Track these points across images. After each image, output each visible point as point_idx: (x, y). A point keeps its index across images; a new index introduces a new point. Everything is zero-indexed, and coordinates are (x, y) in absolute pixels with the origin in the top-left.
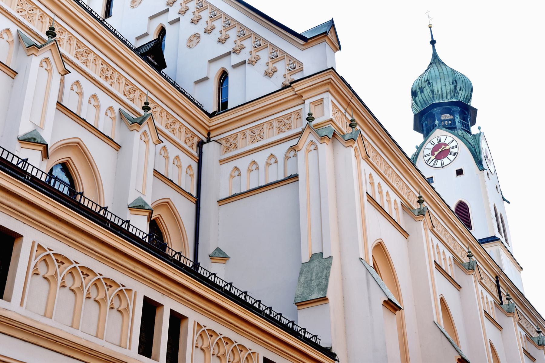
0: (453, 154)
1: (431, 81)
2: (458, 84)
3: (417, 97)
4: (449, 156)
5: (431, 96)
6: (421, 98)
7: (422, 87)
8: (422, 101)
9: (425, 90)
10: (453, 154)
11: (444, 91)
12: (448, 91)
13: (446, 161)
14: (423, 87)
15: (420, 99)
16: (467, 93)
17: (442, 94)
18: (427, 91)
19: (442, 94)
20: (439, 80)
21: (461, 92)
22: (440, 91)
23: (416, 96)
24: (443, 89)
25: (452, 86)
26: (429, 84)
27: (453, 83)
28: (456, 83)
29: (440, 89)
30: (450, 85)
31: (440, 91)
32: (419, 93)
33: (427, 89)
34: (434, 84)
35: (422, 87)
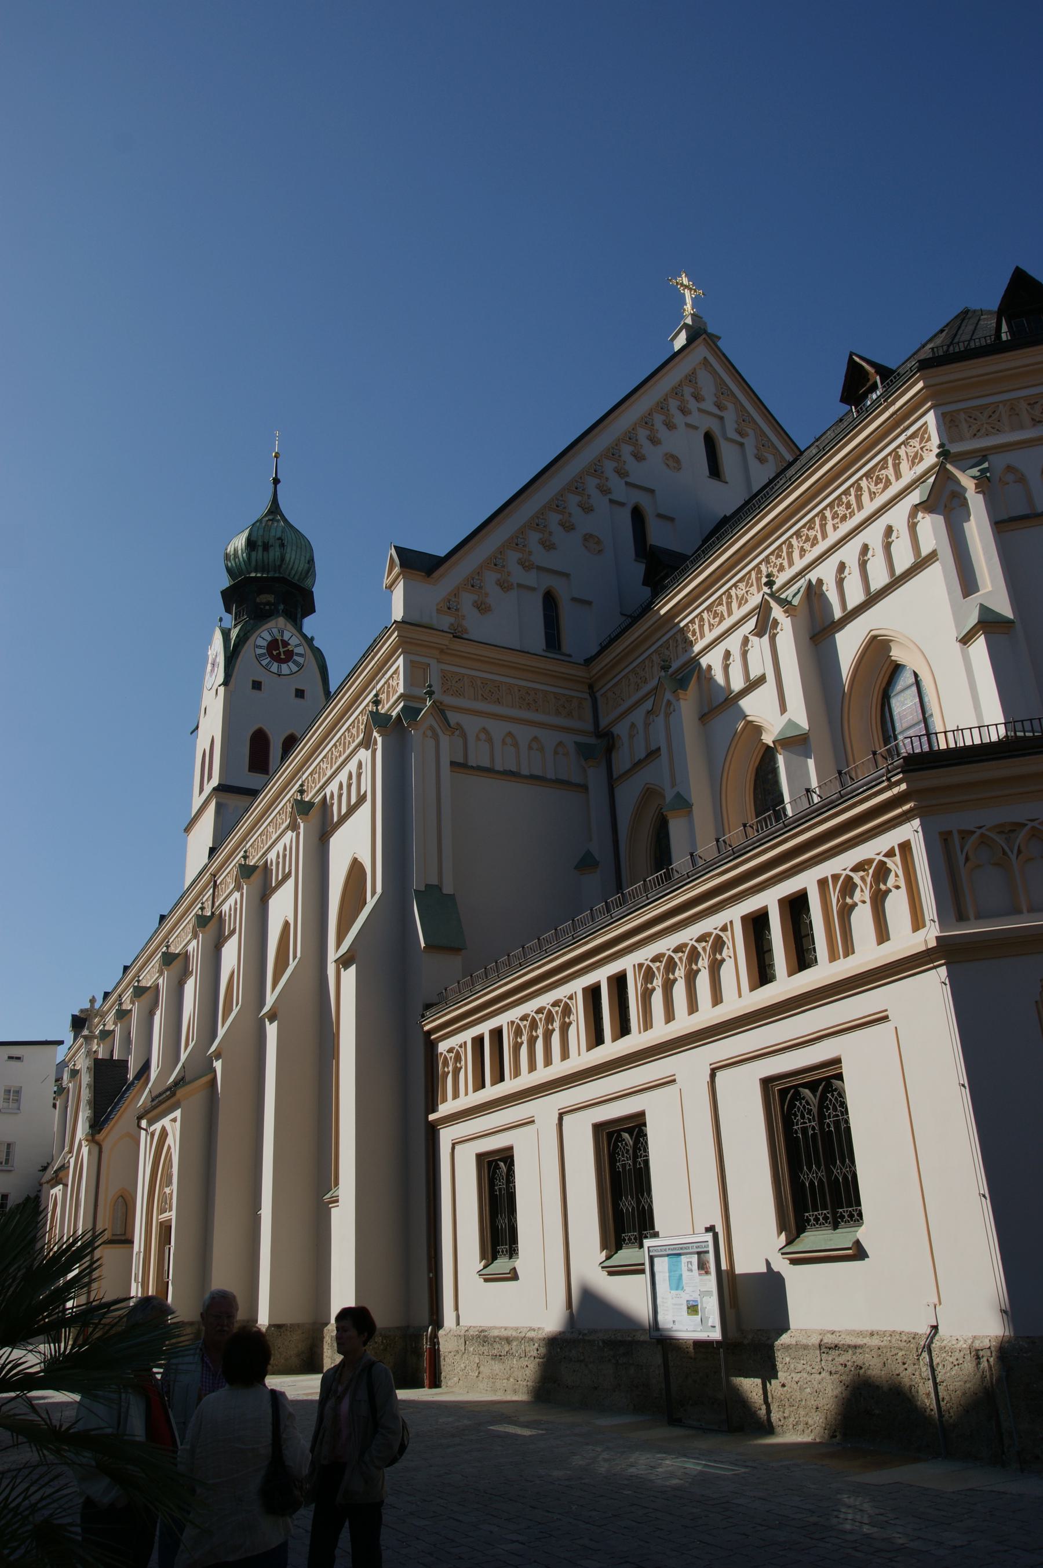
0: (296, 663)
4: (290, 664)
5: (278, 563)
6: (261, 557)
9: (271, 550)
10: (296, 663)
11: (296, 567)
12: (300, 569)
13: (285, 669)
14: (270, 543)
15: (258, 558)
17: (292, 568)
18: (274, 553)
19: (292, 568)
20: (294, 548)
22: (291, 563)
25: (307, 565)
26: (282, 545)
27: (309, 562)
29: (292, 560)
30: (305, 562)
31: (291, 563)
35: (268, 542)
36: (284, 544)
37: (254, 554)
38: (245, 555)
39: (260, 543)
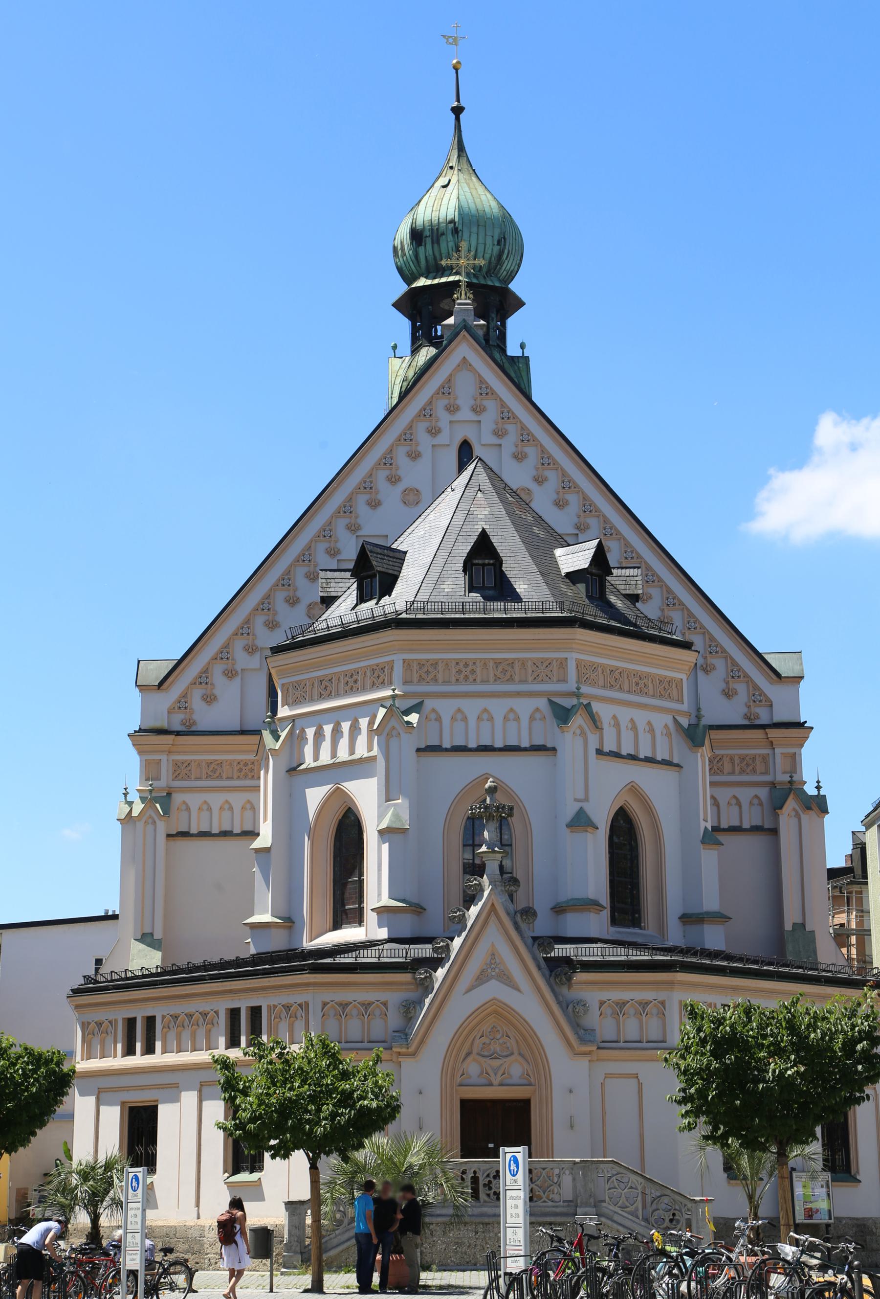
1: (460, 228)
2: (507, 247)
3: (423, 247)
7: (437, 229)
8: (431, 258)
15: (427, 254)
16: (514, 265)
20: (474, 229)
21: (506, 262)
23: (421, 245)
24: (479, 250)
27: (499, 243)
28: (505, 245)
30: (494, 245)
32: (429, 241)
33: (449, 240)
34: (466, 235)
36: (457, 228)
37: (421, 250)
38: (411, 252)
39: (427, 233)
